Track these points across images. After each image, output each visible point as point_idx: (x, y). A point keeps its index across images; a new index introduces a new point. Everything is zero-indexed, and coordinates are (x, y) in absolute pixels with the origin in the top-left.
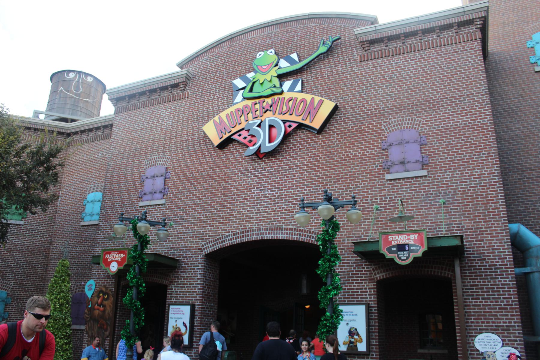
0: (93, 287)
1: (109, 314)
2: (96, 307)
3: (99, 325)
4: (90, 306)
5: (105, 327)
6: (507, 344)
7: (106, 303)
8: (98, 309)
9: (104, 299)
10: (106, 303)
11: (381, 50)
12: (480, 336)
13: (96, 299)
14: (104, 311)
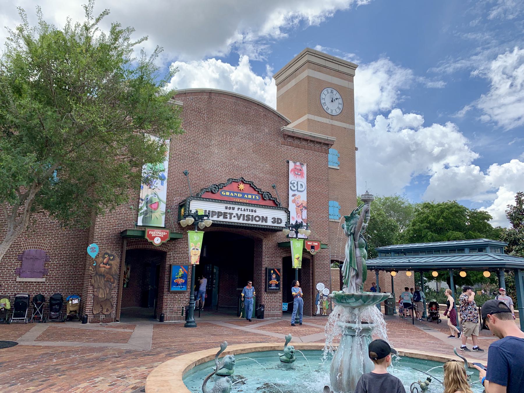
0: (97, 250)
1: (115, 271)
2: (102, 265)
3: (105, 279)
4: (94, 265)
5: (112, 280)
6: (326, 287)
7: (110, 262)
8: (104, 267)
9: (109, 259)
10: (110, 262)
11: (291, 142)
12: (318, 284)
13: (101, 259)
14: (110, 269)
